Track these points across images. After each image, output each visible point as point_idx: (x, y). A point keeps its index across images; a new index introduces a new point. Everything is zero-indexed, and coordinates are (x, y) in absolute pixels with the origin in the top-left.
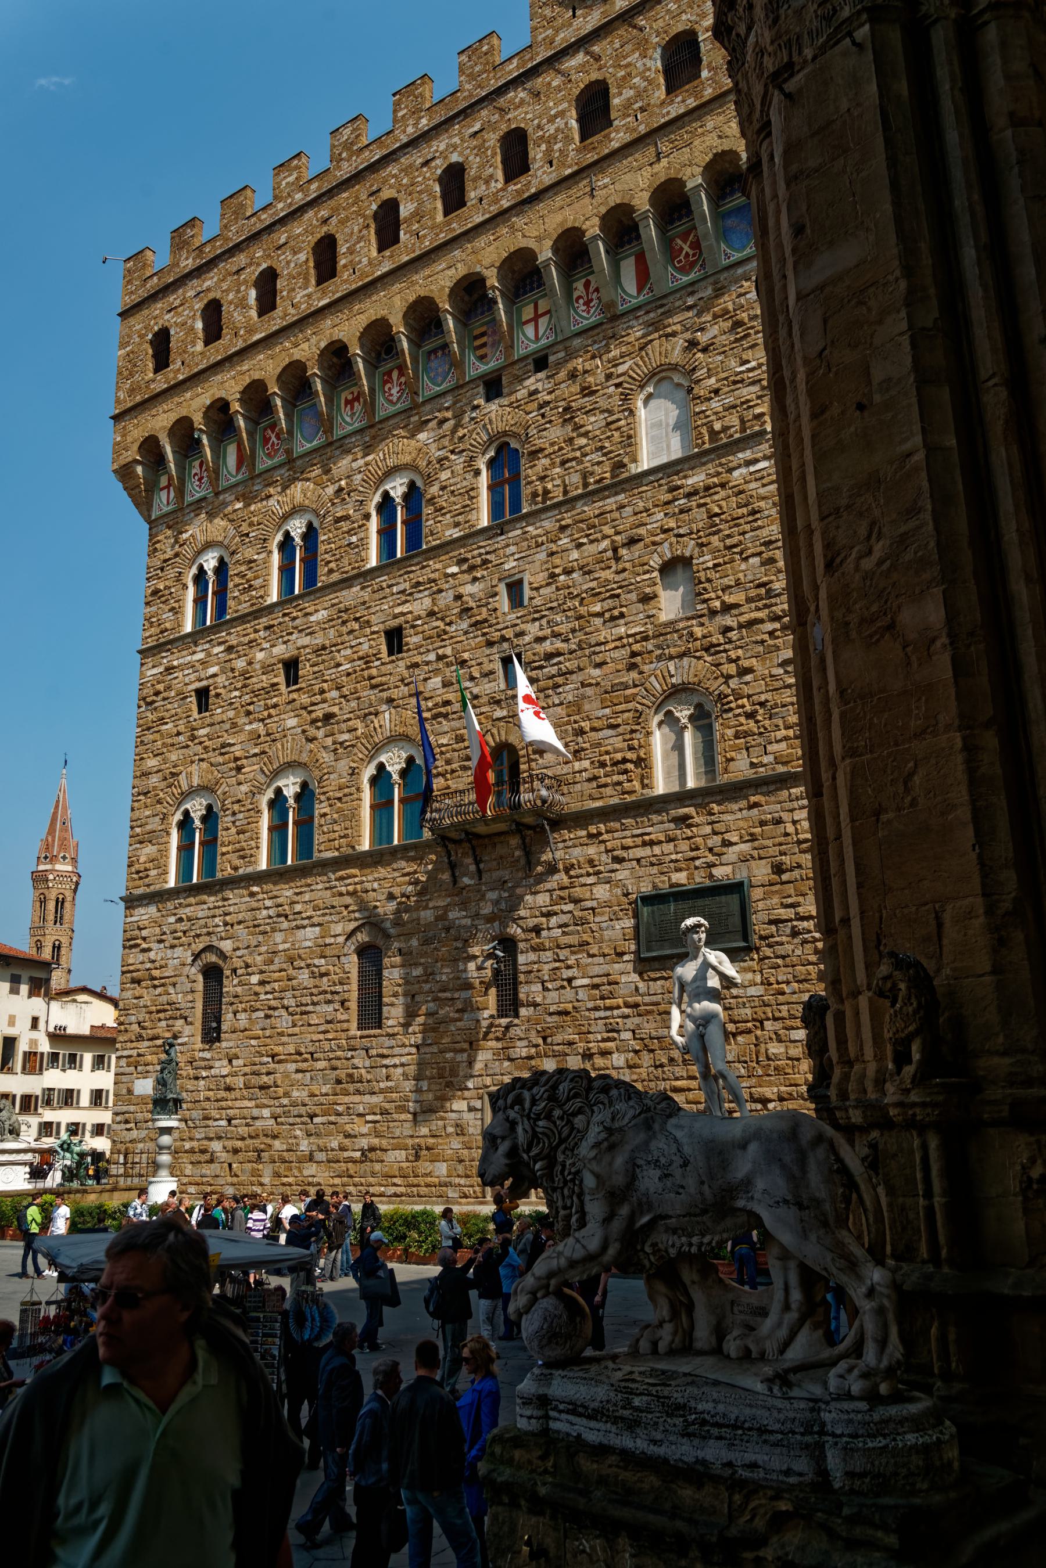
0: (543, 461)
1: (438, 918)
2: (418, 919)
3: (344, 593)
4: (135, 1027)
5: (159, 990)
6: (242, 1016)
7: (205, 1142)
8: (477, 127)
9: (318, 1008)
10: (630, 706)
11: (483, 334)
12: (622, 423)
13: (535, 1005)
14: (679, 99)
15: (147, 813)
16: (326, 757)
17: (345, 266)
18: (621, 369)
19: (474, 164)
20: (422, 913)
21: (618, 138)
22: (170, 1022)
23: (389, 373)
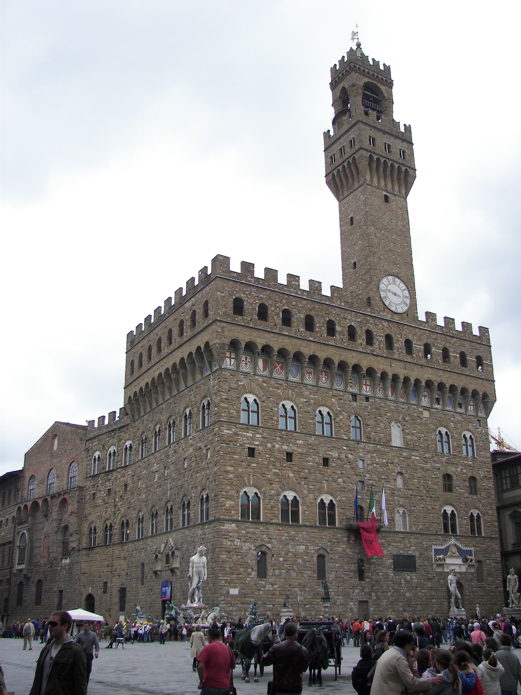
1: (343, 551)
2: (337, 550)
3: (309, 438)
4: (228, 569)
5: (239, 557)
6: (277, 572)
7: (264, 612)
8: (359, 320)
9: (305, 572)
10: (392, 506)
11: (351, 379)
13: (370, 578)
15: (228, 488)
16: (306, 492)
17: (318, 331)
18: (388, 415)
20: (339, 549)
22: (246, 569)
23: (322, 372)
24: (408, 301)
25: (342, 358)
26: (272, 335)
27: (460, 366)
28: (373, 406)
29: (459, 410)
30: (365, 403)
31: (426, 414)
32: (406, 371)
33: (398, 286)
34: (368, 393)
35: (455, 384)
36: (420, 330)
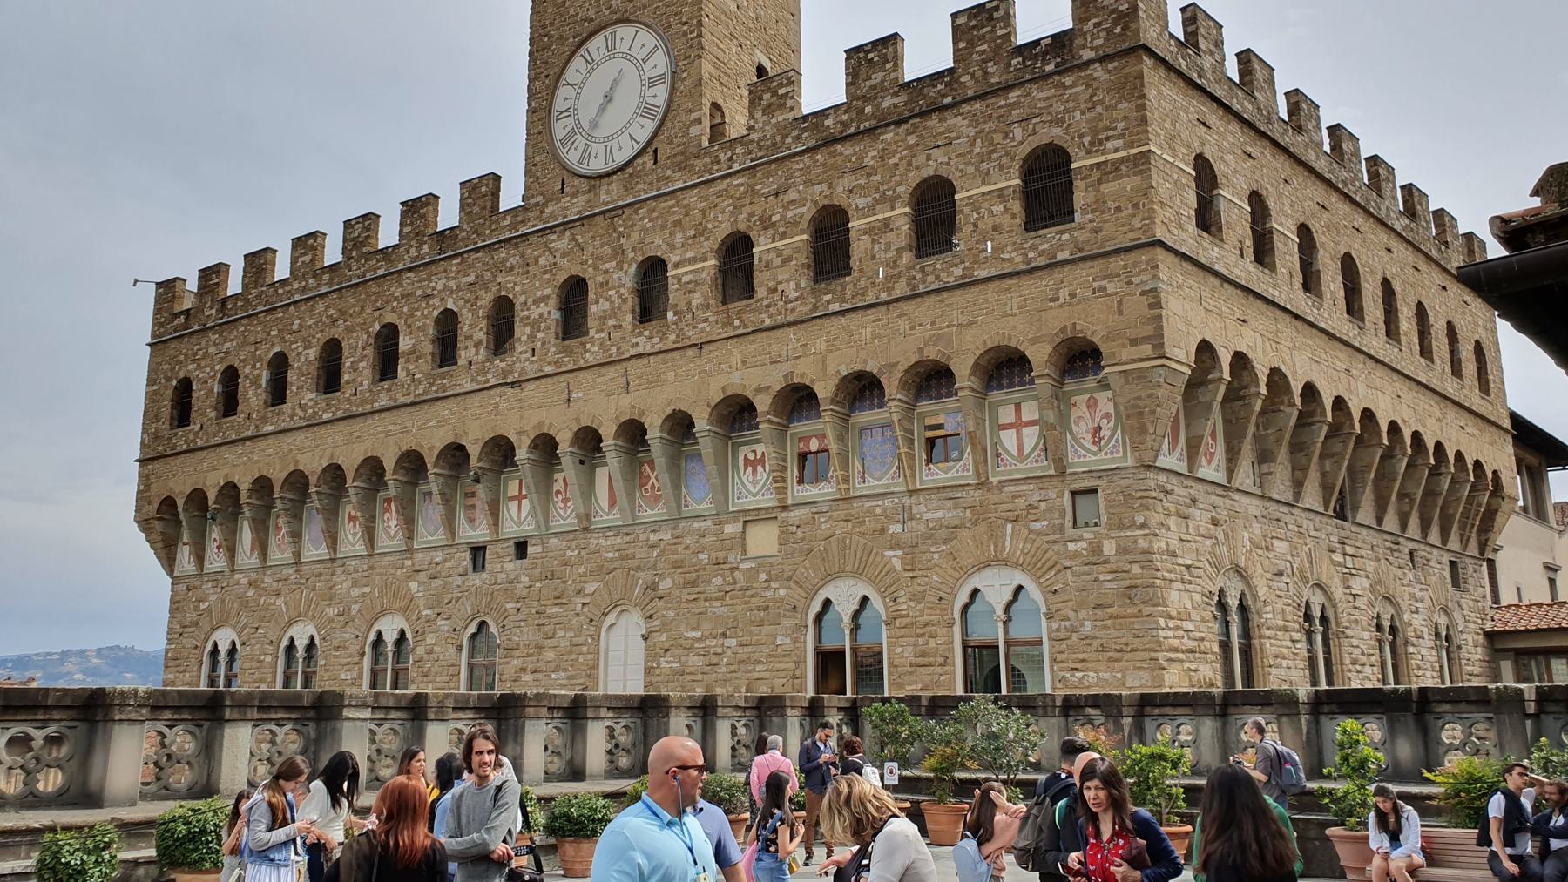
0: (515, 662)
8: (471, 279)
12: (585, 649)
14: (647, 333)
17: (348, 382)
18: (590, 588)
19: (466, 318)
21: (593, 354)
23: (388, 501)
24: (659, 96)
25: (408, 443)
26: (240, 448)
27: (907, 258)
28: (537, 572)
29: (938, 474)
30: (509, 566)
31: (763, 540)
32: (626, 400)
33: (627, 56)
34: (524, 527)
35: (872, 367)
36: (704, 190)
